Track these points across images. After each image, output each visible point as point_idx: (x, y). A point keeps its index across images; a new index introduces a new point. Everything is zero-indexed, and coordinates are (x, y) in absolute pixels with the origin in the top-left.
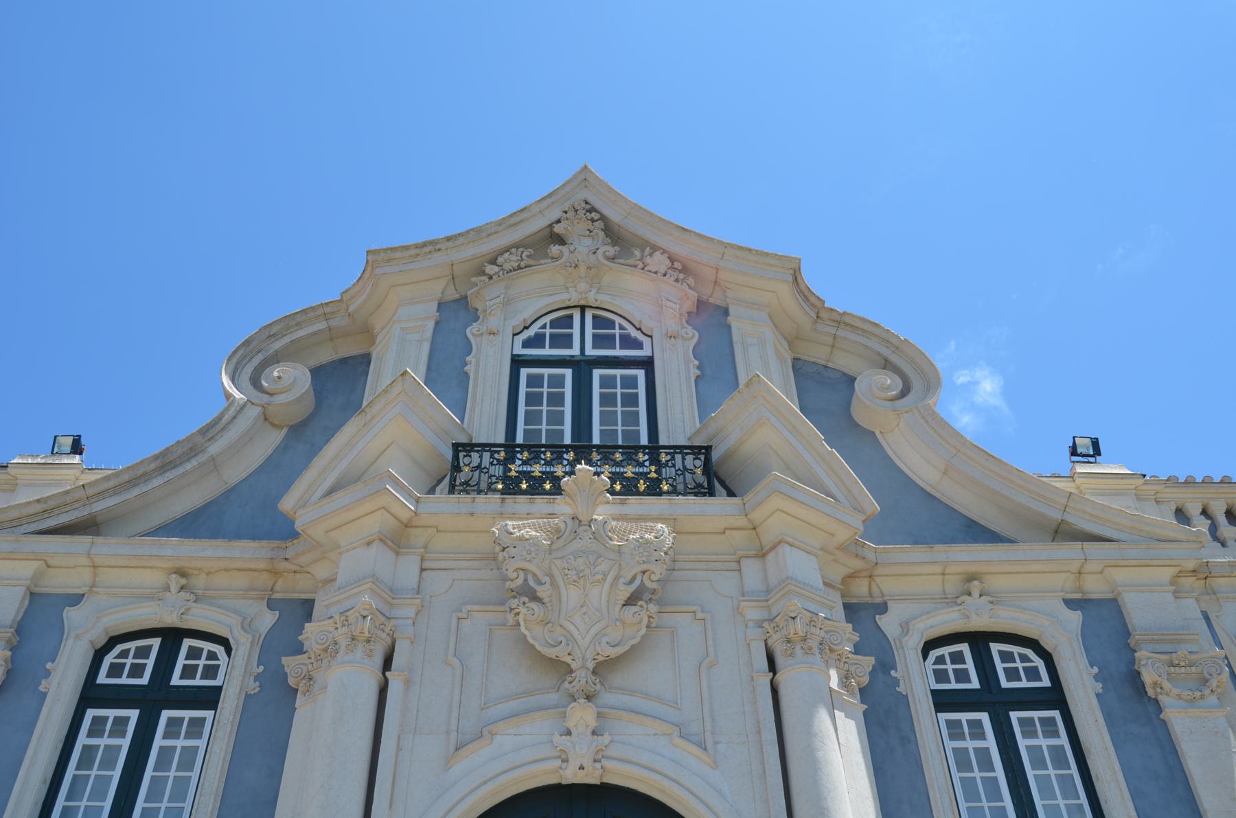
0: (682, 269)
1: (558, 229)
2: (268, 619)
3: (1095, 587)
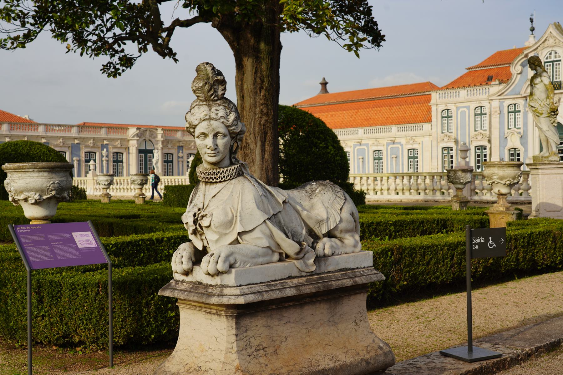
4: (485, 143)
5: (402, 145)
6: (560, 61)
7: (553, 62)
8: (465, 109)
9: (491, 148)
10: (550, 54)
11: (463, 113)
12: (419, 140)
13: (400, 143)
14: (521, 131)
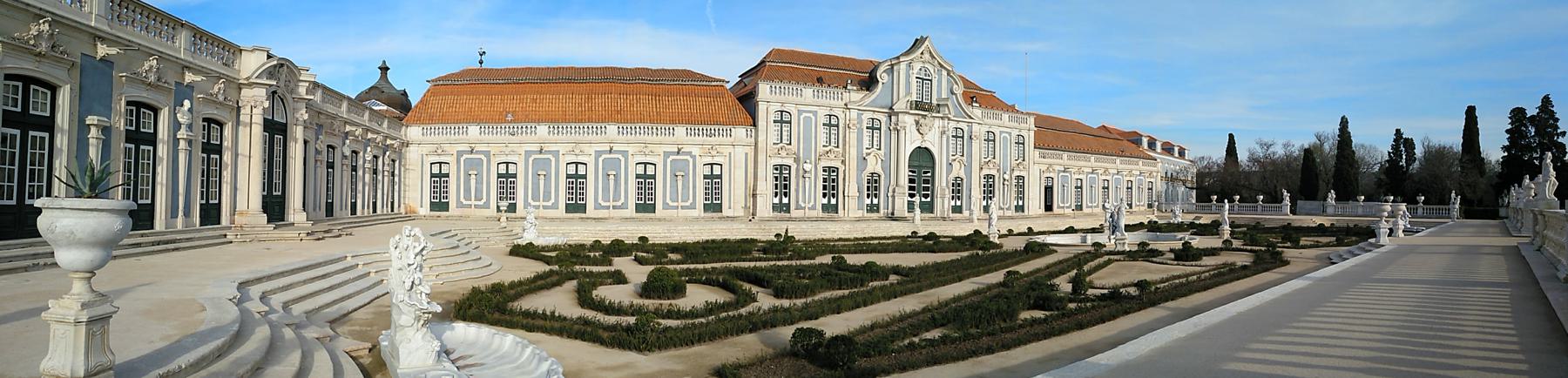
5: (694, 157)
6: (931, 80)
7: (923, 79)
8: (811, 115)
10: (921, 69)
12: (726, 150)
13: (689, 153)
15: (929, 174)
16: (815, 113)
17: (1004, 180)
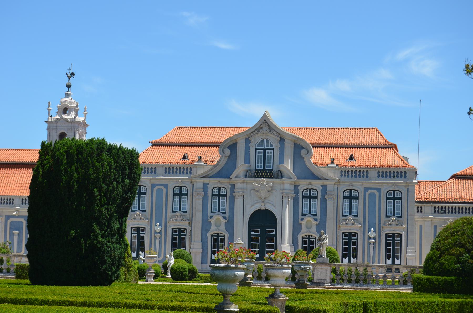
0: (279, 134)
1: (261, 126)
2: (230, 186)
3: (325, 184)
4: (183, 225)
6: (273, 149)
7: (265, 150)
8: (162, 187)
9: (191, 231)
10: (262, 141)
11: (159, 191)
14: (227, 215)
15: (273, 233)
16: (166, 186)
17: (370, 238)
